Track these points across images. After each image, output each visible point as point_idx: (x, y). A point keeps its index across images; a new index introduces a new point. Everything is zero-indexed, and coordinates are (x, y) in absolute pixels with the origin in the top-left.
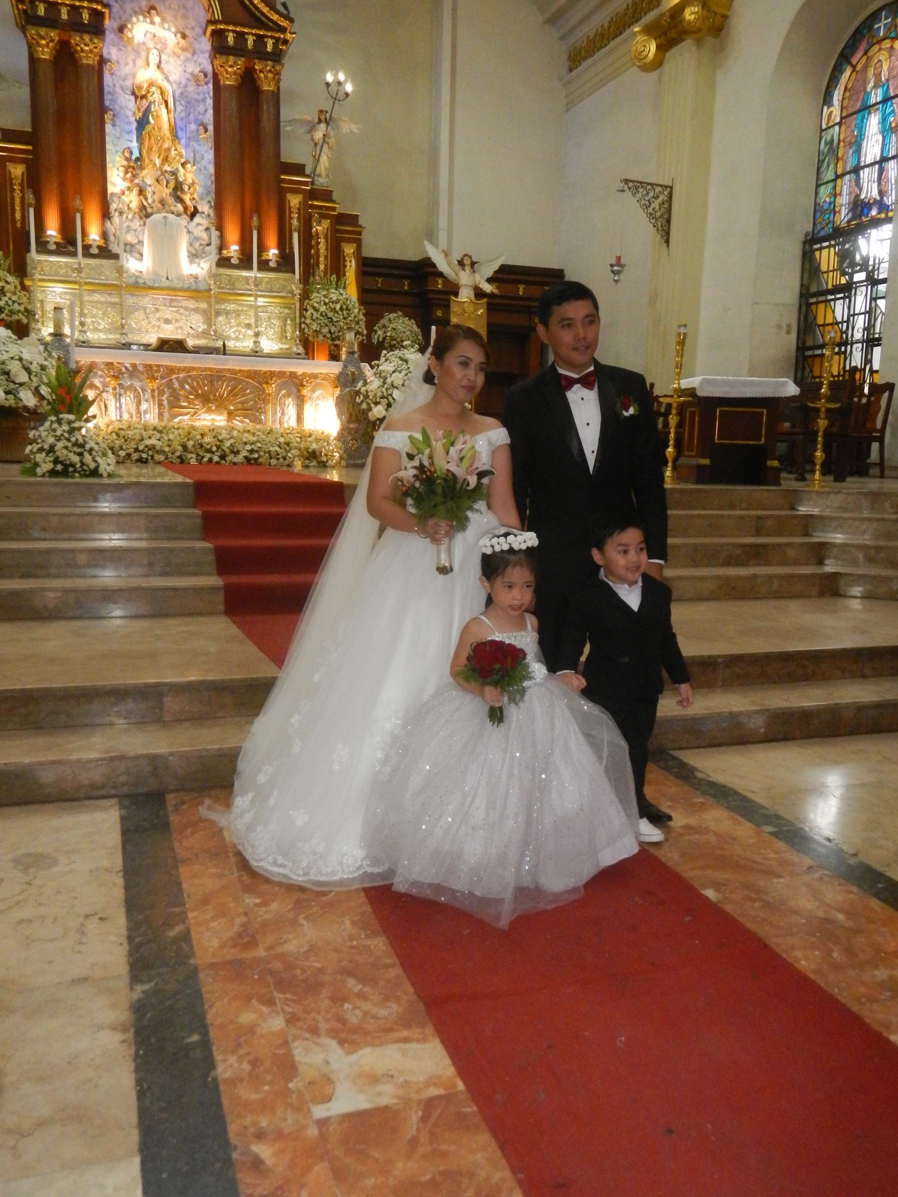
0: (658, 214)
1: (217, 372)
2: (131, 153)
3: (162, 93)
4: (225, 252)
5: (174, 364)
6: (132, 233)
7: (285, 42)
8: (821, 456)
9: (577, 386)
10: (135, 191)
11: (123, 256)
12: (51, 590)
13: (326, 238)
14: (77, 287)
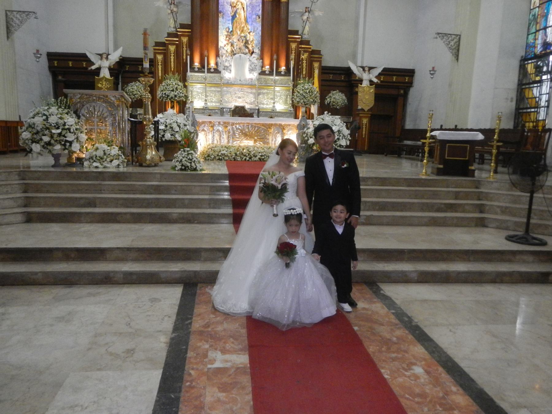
0: (454, 47)
2: (229, 29)
3: (242, 4)
4: (264, 68)
6: (228, 62)
8: (494, 166)
9: (328, 158)
10: (230, 45)
11: (223, 72)
12: (174, 213)
13: (306, 61)
14: (204, 85)
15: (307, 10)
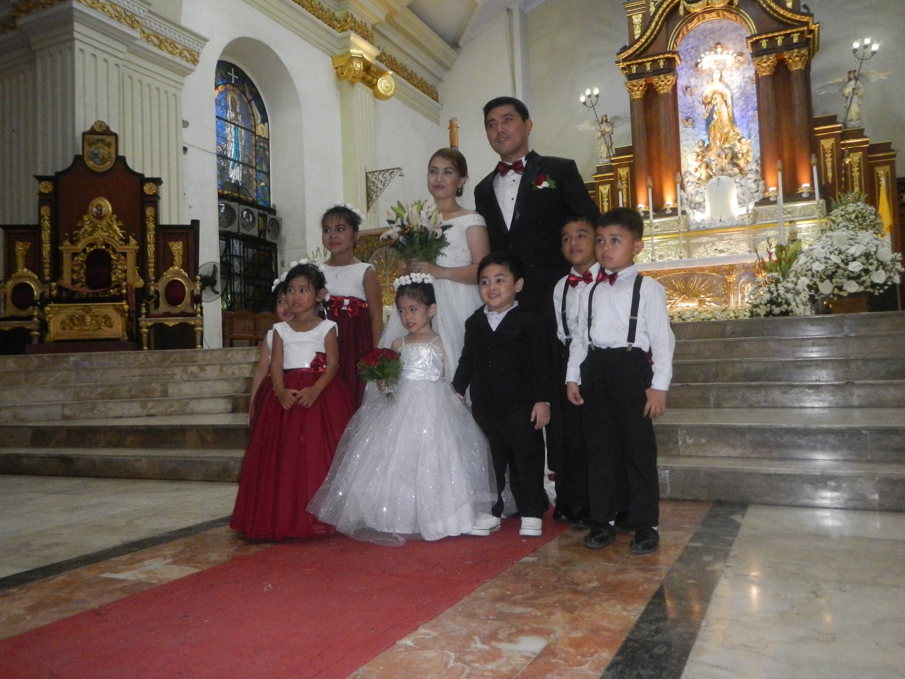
1: (690, 271)
2: (704, 142)
4: (767, 194)
5: (657, 270)
6: (700, 195)
7: (811, 32)
10: (703, 167)
13: (859, 166)
15: (852, 76)
